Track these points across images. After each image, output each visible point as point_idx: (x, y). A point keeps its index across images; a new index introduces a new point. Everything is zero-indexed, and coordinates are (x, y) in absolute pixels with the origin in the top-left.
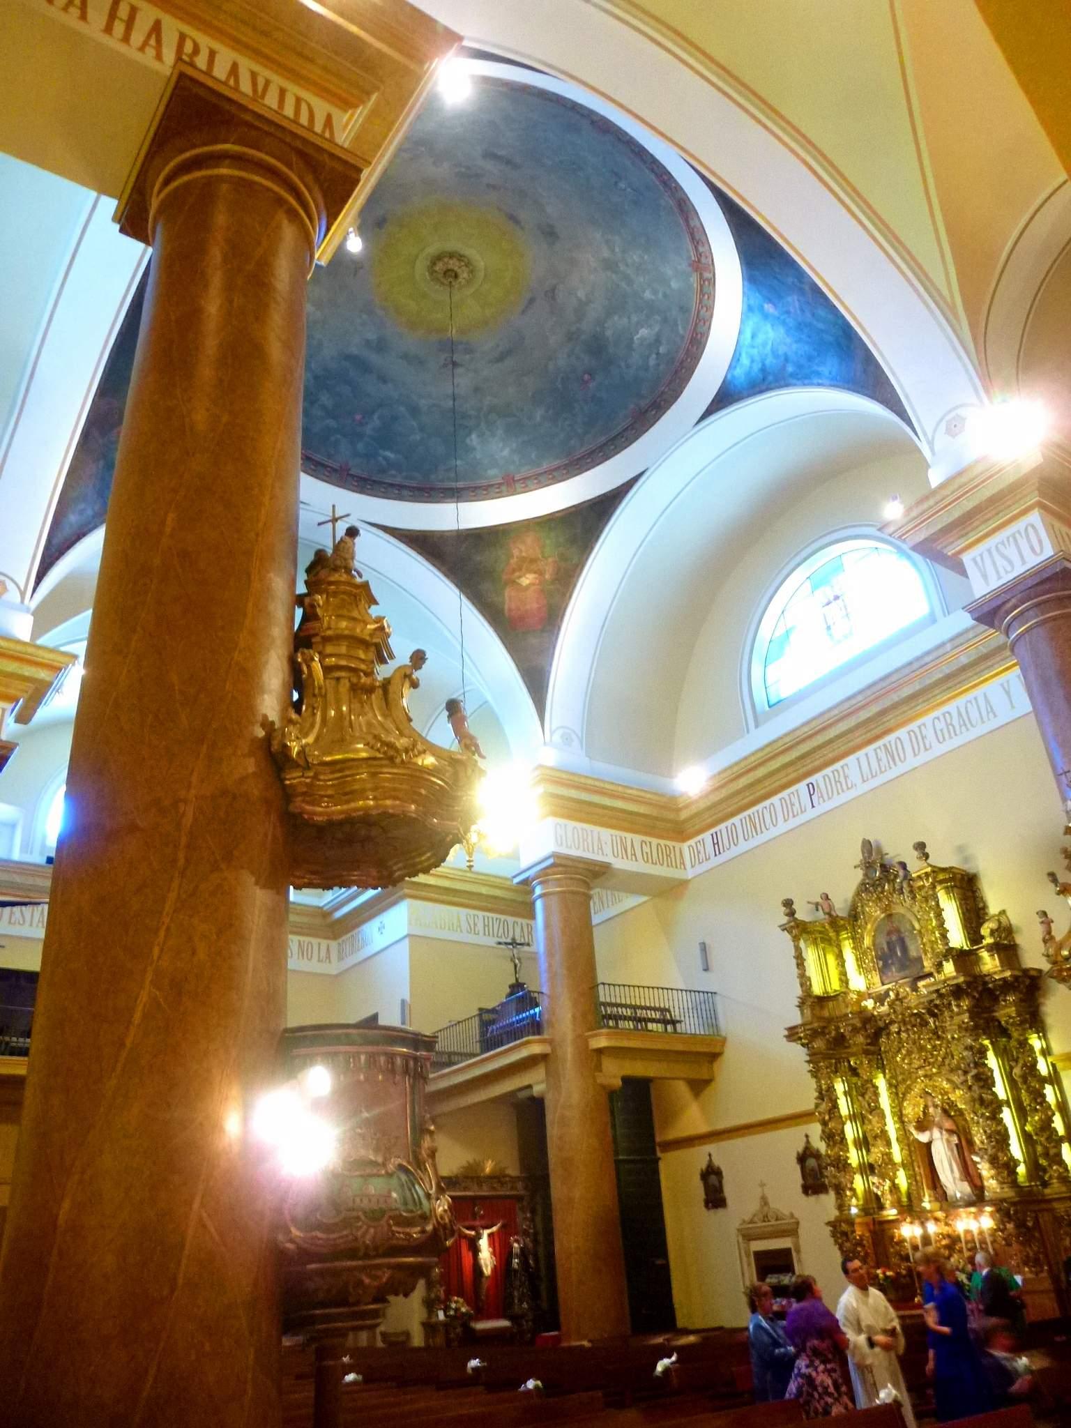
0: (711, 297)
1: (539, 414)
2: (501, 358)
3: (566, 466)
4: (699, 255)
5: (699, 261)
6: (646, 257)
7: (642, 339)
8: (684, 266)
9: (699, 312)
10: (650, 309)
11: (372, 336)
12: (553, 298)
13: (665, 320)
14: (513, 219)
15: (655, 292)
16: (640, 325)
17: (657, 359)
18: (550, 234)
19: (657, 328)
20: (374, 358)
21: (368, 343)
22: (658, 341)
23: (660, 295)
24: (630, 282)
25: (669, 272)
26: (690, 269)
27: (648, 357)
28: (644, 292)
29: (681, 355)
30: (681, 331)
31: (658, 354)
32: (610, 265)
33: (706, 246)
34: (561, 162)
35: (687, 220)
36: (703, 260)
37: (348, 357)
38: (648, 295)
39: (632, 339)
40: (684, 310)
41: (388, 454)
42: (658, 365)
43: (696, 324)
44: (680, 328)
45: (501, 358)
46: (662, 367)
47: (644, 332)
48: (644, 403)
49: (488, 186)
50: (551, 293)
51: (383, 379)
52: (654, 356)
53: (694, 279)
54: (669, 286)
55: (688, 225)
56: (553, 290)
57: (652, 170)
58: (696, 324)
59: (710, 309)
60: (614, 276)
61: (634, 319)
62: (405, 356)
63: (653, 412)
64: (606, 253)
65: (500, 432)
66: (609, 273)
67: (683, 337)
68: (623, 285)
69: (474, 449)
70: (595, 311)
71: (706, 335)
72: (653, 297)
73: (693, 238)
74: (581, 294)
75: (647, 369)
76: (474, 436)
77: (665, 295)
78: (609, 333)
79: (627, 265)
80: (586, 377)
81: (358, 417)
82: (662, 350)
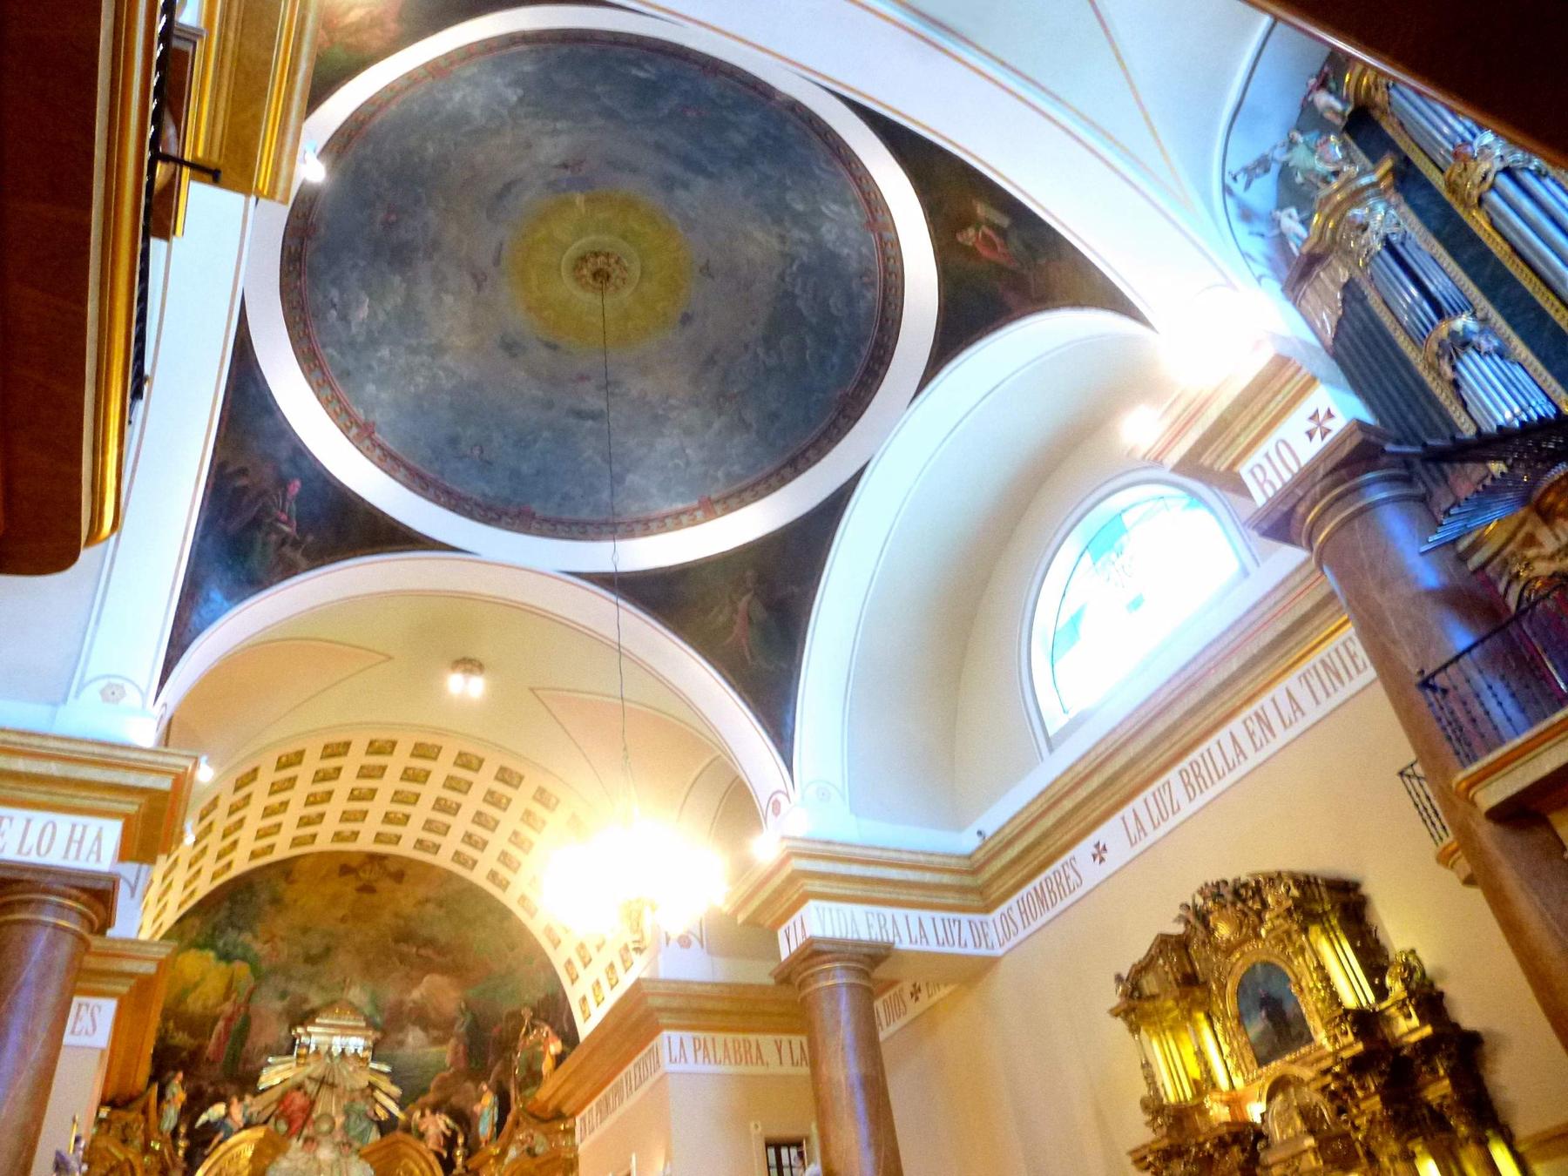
0: (334, 416)
1: (431, 149)
2: (508, 187)
3: (363, 123)
4: (376, 445)
5: (370, 437)
6: (412, 389)
7: (359, 303)
8: (377, 417)
9: (332, 389)
10: (373, 342)
11: (680, 194)
12: (474, 276)
13: (352, 344)
14: (552, 347)
15: (381, 361)
16: (373, 315)
17: (332, 301)
18: (511, 347)
19: (354, 330)
20: (675, 170)
21: (686, 186)
22: (344, 318)
23: (374, 364)
24: (413, 351)
25: (384, 396)
26: (371, 418)
27: (341, 294)
28: (391, 351)
29: (313, 331)
30: (330, 350)
31: (334, 306)
32: (438, 350)
33: (376, 460)
34: (535, 441)
35: (408, 468)
36: (367, 443)
37: (710, 176)
38: (385, 352)
39: (370, 296)
40: (345, 374)
41: (642, 74)
42: (325, 297)
43: (324, 374)
44: (335, 353)
45: (508, 187)
46: (320, 298)
47: (363, 313)
48: (311, 246)
49: (588, 378)
50: (479, 279)
51: (659, 147)
52: (336, 300)
53: (359, 413)
54: (374, 382)
55: (408, 468)
56: (479, 287)
57: (466, 500)
58: (324, 374)
59: (325, 403)
60: (426, 342)
61: (382, 317)
62: (634, 170)
63: (293, 249)
64: (448, 360)
65: (476, 112)
66: (433, 341)
67: (324, 346)
68: (414, 342)
69: (509, 85)
70: (425, 291)
71: (307, 372)
72: (379, 354)
73: (394, 458)
74: (448, 299)
75: (333, 282)
76: (514, 99)
77: (370, 368)
78: (397, 279)
79: (423, 365)
80: (393, 218)
81: (691, 114)
82: (334, 313)
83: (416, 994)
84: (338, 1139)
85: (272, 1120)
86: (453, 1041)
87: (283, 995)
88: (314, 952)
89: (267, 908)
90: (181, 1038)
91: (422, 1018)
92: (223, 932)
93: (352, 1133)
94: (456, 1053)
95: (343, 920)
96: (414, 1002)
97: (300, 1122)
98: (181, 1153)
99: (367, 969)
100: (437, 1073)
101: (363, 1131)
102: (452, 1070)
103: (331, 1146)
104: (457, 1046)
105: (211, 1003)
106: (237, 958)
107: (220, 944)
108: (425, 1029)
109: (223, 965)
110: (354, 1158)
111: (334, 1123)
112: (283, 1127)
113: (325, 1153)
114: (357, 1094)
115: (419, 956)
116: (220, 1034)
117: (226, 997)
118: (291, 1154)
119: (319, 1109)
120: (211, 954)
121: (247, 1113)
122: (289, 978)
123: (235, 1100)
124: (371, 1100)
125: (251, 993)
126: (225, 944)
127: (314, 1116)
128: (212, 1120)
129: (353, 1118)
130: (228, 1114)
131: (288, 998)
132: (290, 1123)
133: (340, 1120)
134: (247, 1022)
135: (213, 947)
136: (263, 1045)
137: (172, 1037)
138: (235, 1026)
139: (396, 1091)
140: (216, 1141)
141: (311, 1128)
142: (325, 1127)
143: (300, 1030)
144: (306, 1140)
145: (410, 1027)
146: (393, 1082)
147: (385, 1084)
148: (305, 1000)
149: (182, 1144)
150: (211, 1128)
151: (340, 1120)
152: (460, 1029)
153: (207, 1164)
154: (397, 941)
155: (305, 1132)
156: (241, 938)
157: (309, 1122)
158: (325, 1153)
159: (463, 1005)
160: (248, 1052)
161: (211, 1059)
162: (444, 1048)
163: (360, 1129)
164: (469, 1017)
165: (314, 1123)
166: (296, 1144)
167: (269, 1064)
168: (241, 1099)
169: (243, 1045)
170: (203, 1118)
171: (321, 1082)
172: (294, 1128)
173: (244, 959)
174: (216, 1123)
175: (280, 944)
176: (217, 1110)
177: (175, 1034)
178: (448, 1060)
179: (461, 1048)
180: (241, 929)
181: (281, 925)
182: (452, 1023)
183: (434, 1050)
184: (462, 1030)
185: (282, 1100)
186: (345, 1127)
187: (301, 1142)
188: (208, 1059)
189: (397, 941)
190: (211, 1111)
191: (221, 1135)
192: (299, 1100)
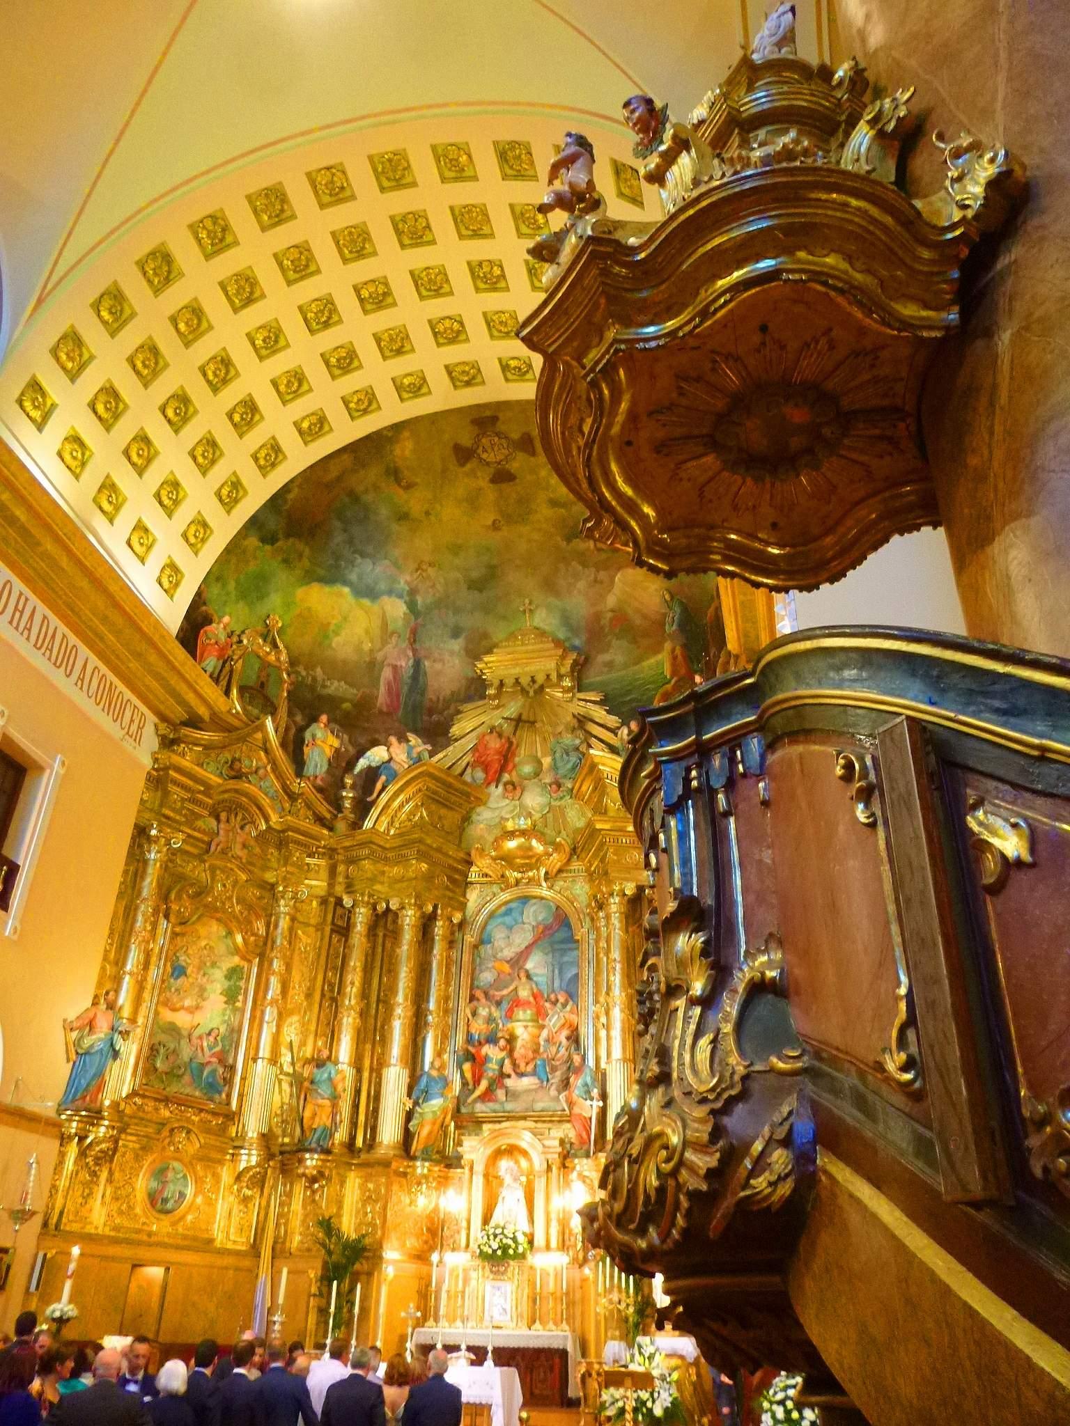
83: (611, 601)
84: (548, 780)
85: (469, 770)
86: (668, 646)
87: (456, 633)
88: (475, 574)
89: (395, 527)
90: (335, 687)
91: (622, 624)
92: (352, 563)
93: (561, 772)
94: (675, 658)
95: (495, 526)
96: (612, 611)
97: (496, 766)
98: (347, 804)
99: (549, 586)
100: (657, 689)
101: (573, 768)
102: (673, 681)
103: (539, 790)
104: (673, 650)
105: (367, 646)
106: (383, 594)
107: (353, 577)
108: (634, 641)
109: (366, 602)
110: (568, 800)
111: (540, 763)
112: (480, 775)
113: (534, 799)
114: (561, 728)
115: (599, 550)
116: (389, 684)
117: (384, 642)
118: (492, 804)
119: (522, 753)
120: (346, 590)
121: (415, 755)
122: (457, 611)
123: (393, 739)
124: (580, 733)
125: (414, 632)
126: (360, 577)
127: (517, 759)
128: (374, 764)
129: (558, 755)
130: (391, 759)
131: (464, 635)
132: (486, 769)
133: (547, 761)
134: (417, 664)
135: (345, 582)
136: (448, 692)
137: (324, 686)
138: (407, 672)
139: (613, 721)
140: (379, 786)
141: (514, 773)
142: (527, 769)
143: (480, 665)
144: (505, 784)
145: (615, 643)
146: (608, 712)
147: (599, 713)
148: (485, 636)
149: (348, 794)
150: (372, 774)
151: (547, 761)
152: (671, 628)
153: (374, 813)
154: (569, 540)
155: (506, 777)
156: (378, 569)
157: (510, 766)
158: (534, 799)
159: (667, 597)
160: (431, 700)
161: (385, 709)
162: (659, 657)
163: (569, 766)
164: (678, 610)
165: (515, 766)
166: (496, 791)
167: (459, 712)
168: (402, 739)
169: (423, 694)
170: (362, 763)
171: (518, 721)
172: (491, 773)
173: (390, 592)
174: (378, 768)
175: (430, 570)
176: (377, 755)
177: (328, 683)
178: (668, 675)
179: (678, 651)
180: (373, 558)
181: (423, 544)
182: (662, 625)
183: (652, 661)
184: (674, 627)
185: (475, 749)
186: (554, 767)
187: (501, 788)
188: (381, 712)
189: (569, 540)
190: (369, 753)
191: (383, 778)
192: (495, 744)
